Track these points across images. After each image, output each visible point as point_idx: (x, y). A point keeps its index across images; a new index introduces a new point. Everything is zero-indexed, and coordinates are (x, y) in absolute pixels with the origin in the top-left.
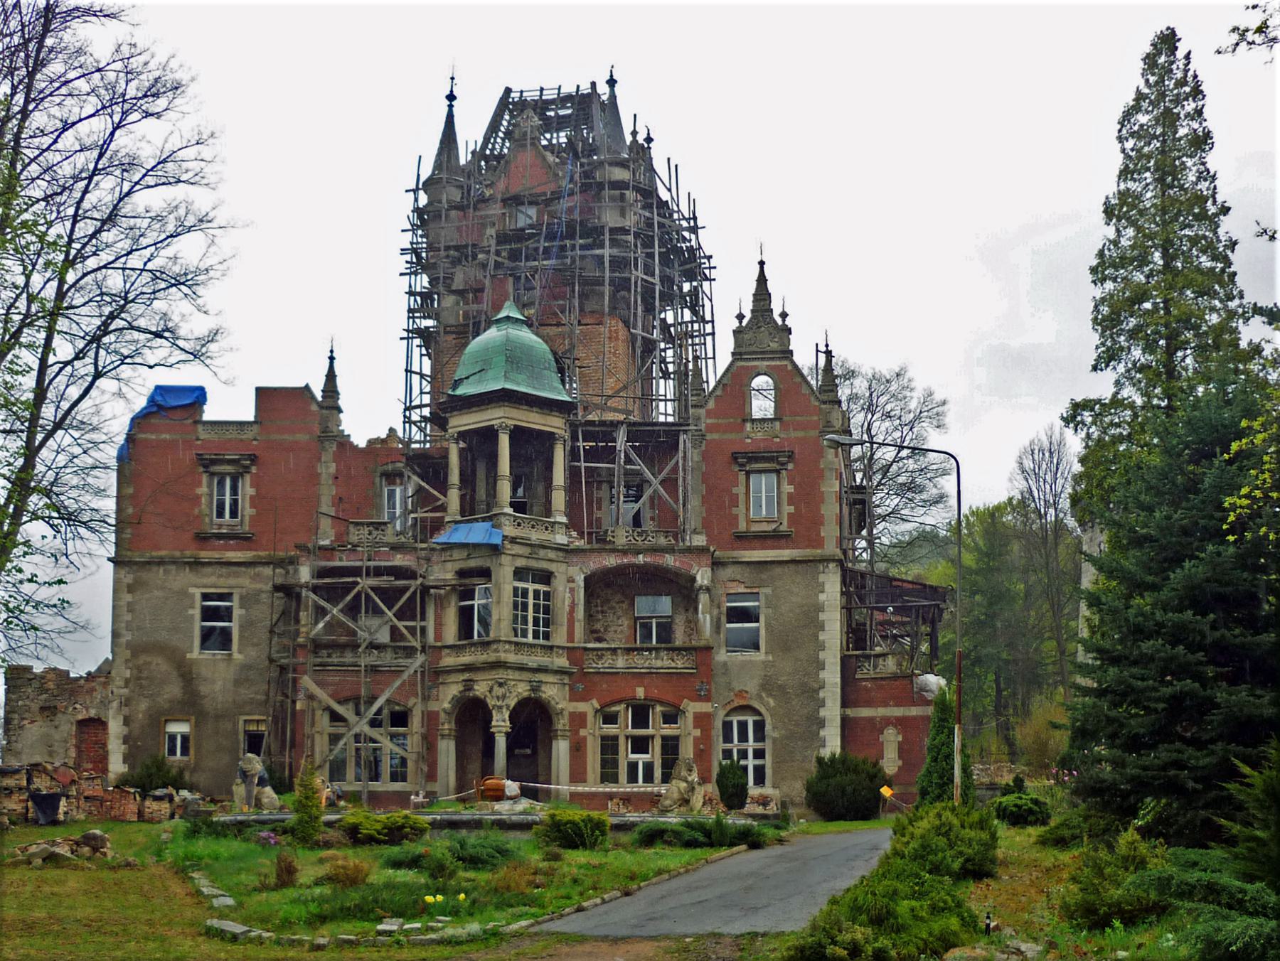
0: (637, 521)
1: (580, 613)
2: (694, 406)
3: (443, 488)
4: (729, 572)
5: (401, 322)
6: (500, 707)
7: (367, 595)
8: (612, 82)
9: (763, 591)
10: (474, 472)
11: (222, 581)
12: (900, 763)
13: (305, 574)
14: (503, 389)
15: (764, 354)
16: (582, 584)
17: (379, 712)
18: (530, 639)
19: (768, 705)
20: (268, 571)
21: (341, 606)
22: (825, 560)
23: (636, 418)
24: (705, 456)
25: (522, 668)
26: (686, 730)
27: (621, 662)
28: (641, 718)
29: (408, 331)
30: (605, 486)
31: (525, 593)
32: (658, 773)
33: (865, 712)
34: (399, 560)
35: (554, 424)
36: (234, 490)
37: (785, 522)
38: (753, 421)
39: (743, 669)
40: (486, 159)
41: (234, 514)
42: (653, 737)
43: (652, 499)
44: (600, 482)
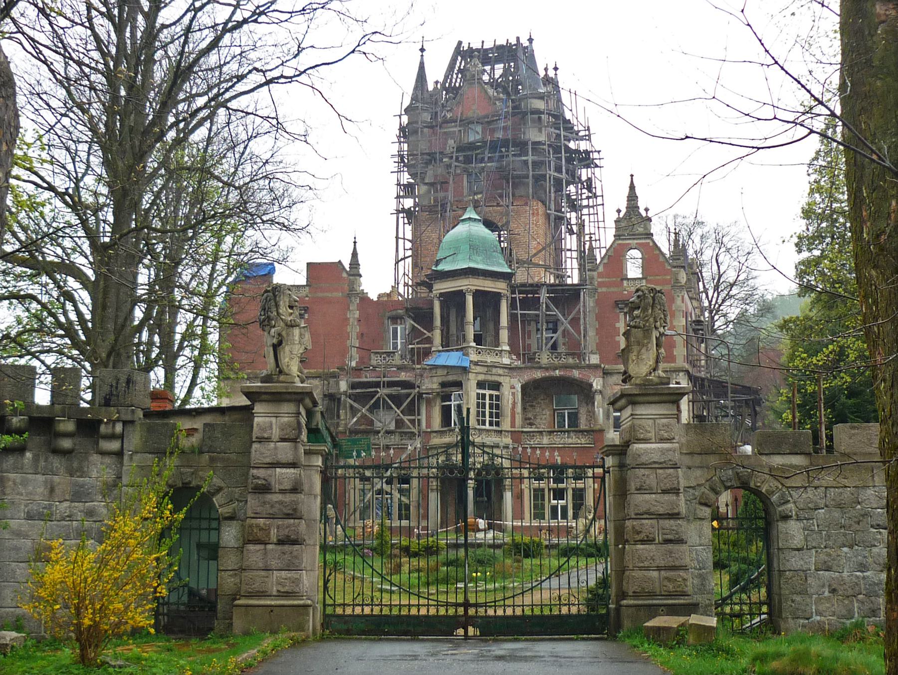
0: (554, 347)
3: (430, 328)
7: (384, 399)
13: (343, 386)
14: (469, 268)
15: (634, 236)
16: (520, 390)
18: (487, 426)
21: (367, 407)
27: (545, 440)
31: (484, 396)
32: (570, 513)
34: (403, 376)
35: (500, 286)
38: (629, 279)
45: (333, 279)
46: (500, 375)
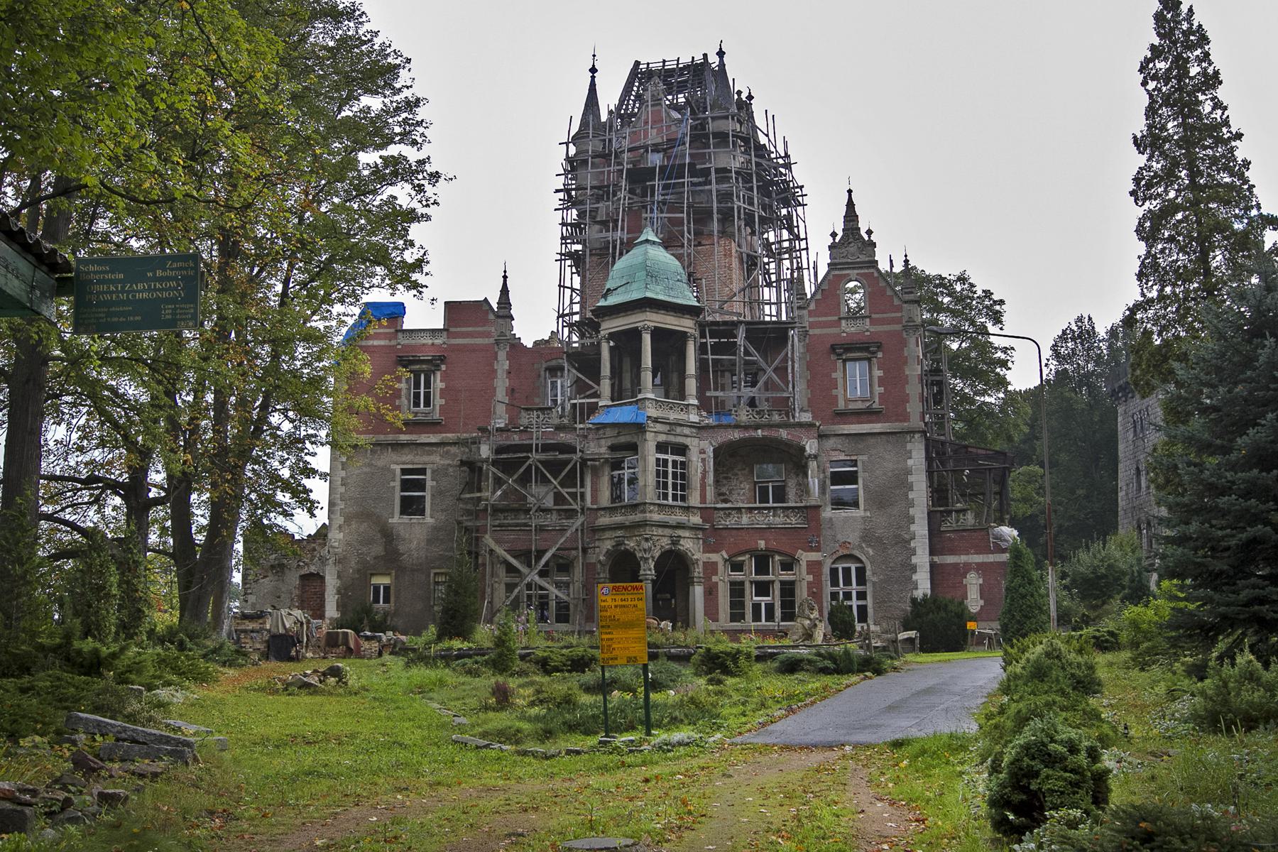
1: (710, 479)
2: (799, 308)
3: (597, 378)
4: (831, 442)
5: (556, 246)
6: (647, 559)
7: (537, 468)
8: (721, 54)
9: (860, 457)
10: (621, 368)
11: (417, 459)
12: (982, 602)
13: (485, 451)
14: (646, 298)
15: (853, 265)
17: (547, 564)
18: (670, 501)
19: (867, 554)
20: (453, 449)
21: (515, 477)
22: (912, 432)
23: (749, 319)
24: (809, 349)
25: (664, 525)
26: (802, 576)
27: (745, 519)
28: (762, 568)
29: (561, 254)
30: (727, 375)
31: (666, 461)
32: (778, 613)
33: (950, 559)
34: (563, 437)
35: (686, 324)
36: (427, 385)
37: (877, 400)
39: (847, 525)
40: (621, 116)
41: (427, 404)
42: (773, 582)
43: (766, 383)
44: (723, 372)
45: (478, 319)
46: (687, 436)
